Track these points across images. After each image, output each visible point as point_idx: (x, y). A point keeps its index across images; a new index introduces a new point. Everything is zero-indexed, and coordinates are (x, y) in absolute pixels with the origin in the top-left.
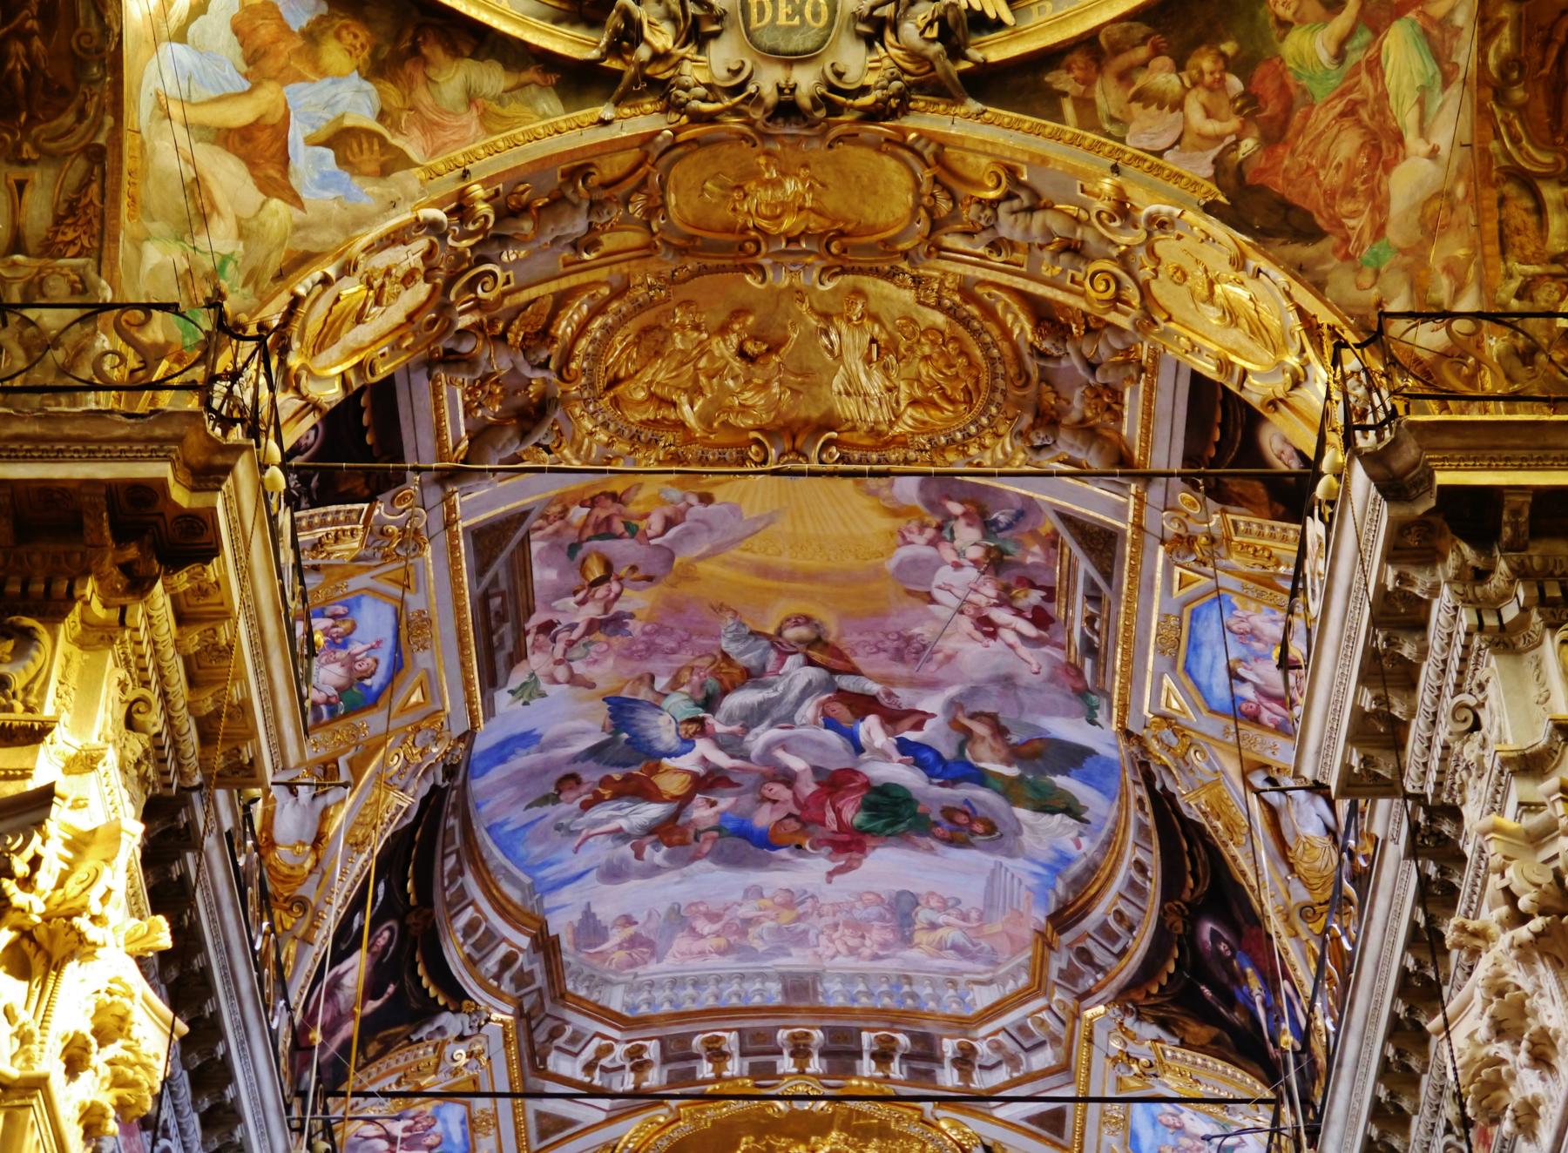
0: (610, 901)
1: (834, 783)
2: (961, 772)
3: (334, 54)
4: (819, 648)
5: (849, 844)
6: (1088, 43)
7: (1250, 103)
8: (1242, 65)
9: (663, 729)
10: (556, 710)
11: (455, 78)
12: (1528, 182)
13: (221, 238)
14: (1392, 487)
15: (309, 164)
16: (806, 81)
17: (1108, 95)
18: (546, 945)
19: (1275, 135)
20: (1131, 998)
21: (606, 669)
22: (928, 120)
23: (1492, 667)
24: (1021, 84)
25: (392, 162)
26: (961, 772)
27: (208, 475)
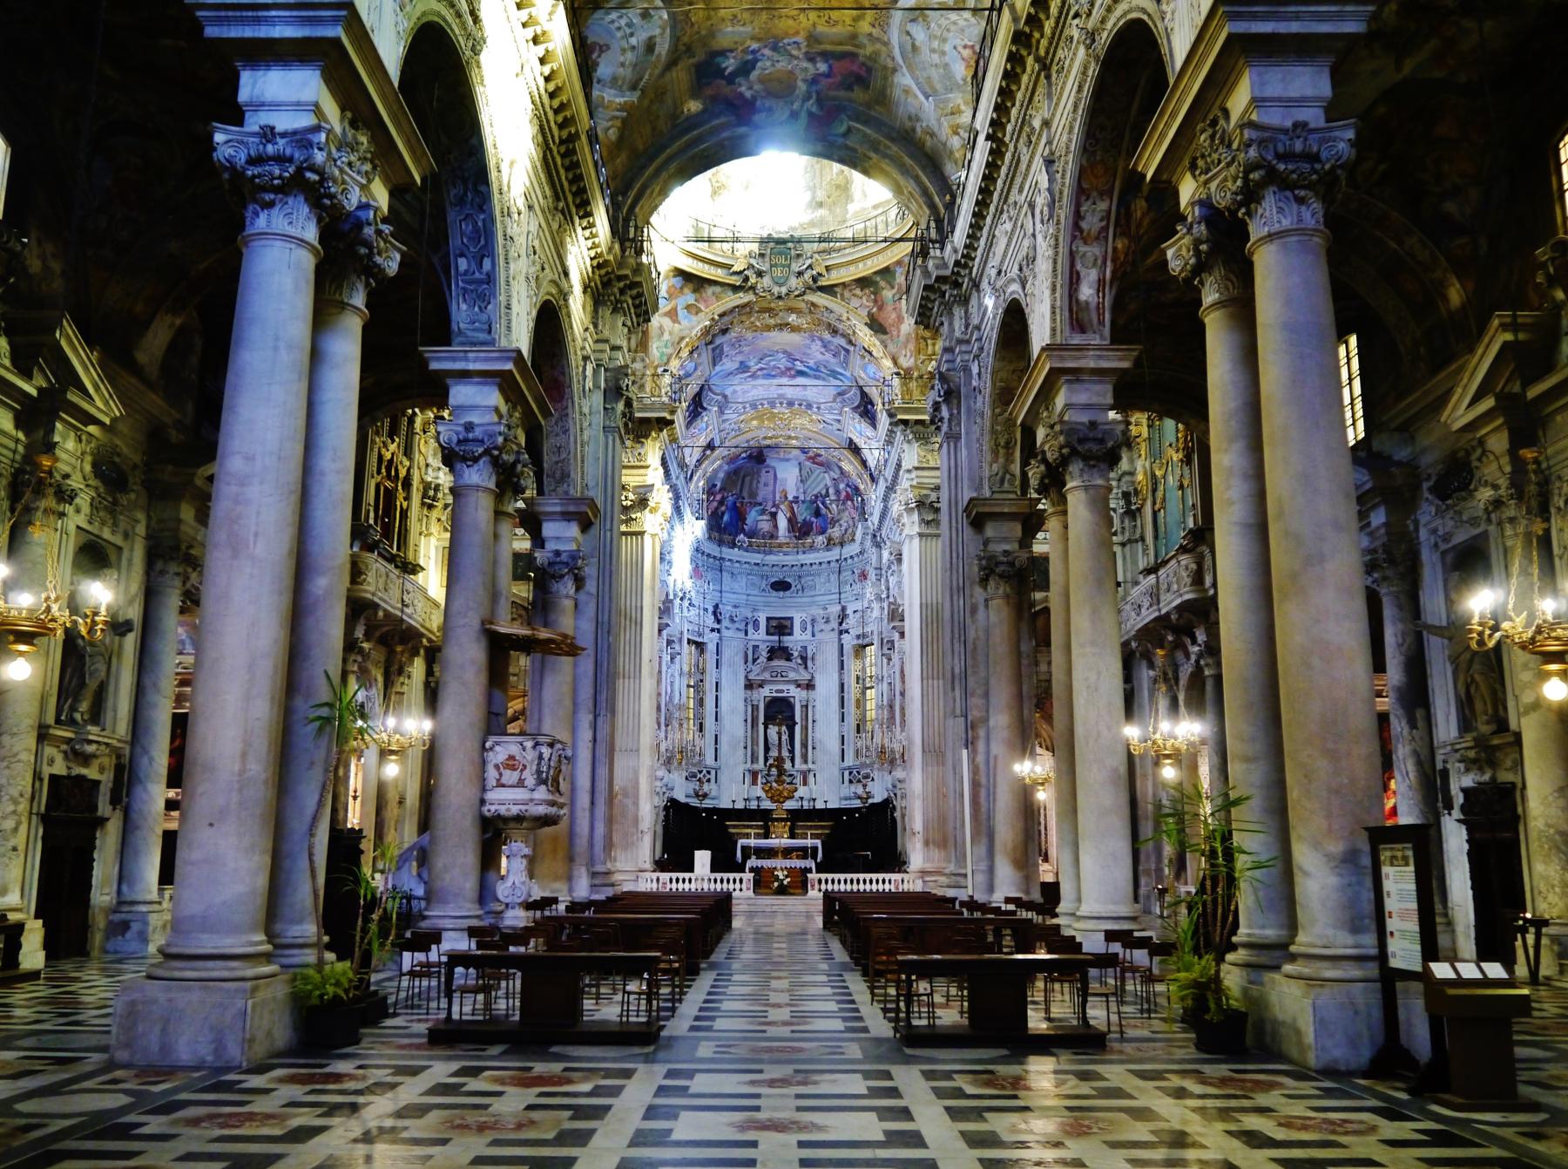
0: (738, 388)
1: (789, 369)
2: (817, 370)
3: (686, 290)
4: (785, 352)
5: (793, 377)
6: (844, 285)
7: (875, 301)
8: (875, 293)
9: (752, 364)
10: (728, 365)
11: (710, 290)
12: (925, 339)
13: (666, 337)
14: (891, 415)
15: (681, 313)
16: (784, 290)
17: (847, 294)
18: (725, 397)
19: (880, 308)
20: (855, 409)
21: (740, 358)
22: (810, 297)
23: (905, 446)
24: (829, 290)
25: (699, 311)
26: (817, 370)
27: (673, 412)
